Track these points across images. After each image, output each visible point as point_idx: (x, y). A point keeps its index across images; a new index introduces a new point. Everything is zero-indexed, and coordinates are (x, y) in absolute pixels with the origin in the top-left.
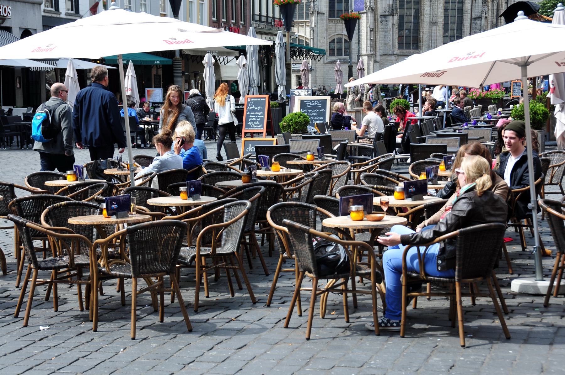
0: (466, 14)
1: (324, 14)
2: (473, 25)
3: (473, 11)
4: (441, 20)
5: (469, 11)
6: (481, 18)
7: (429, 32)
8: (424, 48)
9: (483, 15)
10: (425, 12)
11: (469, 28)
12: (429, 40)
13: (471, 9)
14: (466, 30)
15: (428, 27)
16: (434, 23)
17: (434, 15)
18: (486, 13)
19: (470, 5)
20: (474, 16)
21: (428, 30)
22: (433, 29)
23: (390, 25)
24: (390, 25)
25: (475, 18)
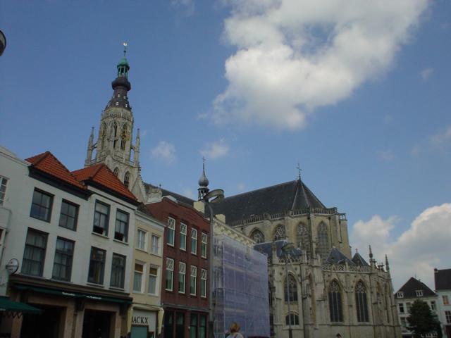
1: (280, 299)
16: (351, 306)
23: (323, 306)
24: (323, 306)
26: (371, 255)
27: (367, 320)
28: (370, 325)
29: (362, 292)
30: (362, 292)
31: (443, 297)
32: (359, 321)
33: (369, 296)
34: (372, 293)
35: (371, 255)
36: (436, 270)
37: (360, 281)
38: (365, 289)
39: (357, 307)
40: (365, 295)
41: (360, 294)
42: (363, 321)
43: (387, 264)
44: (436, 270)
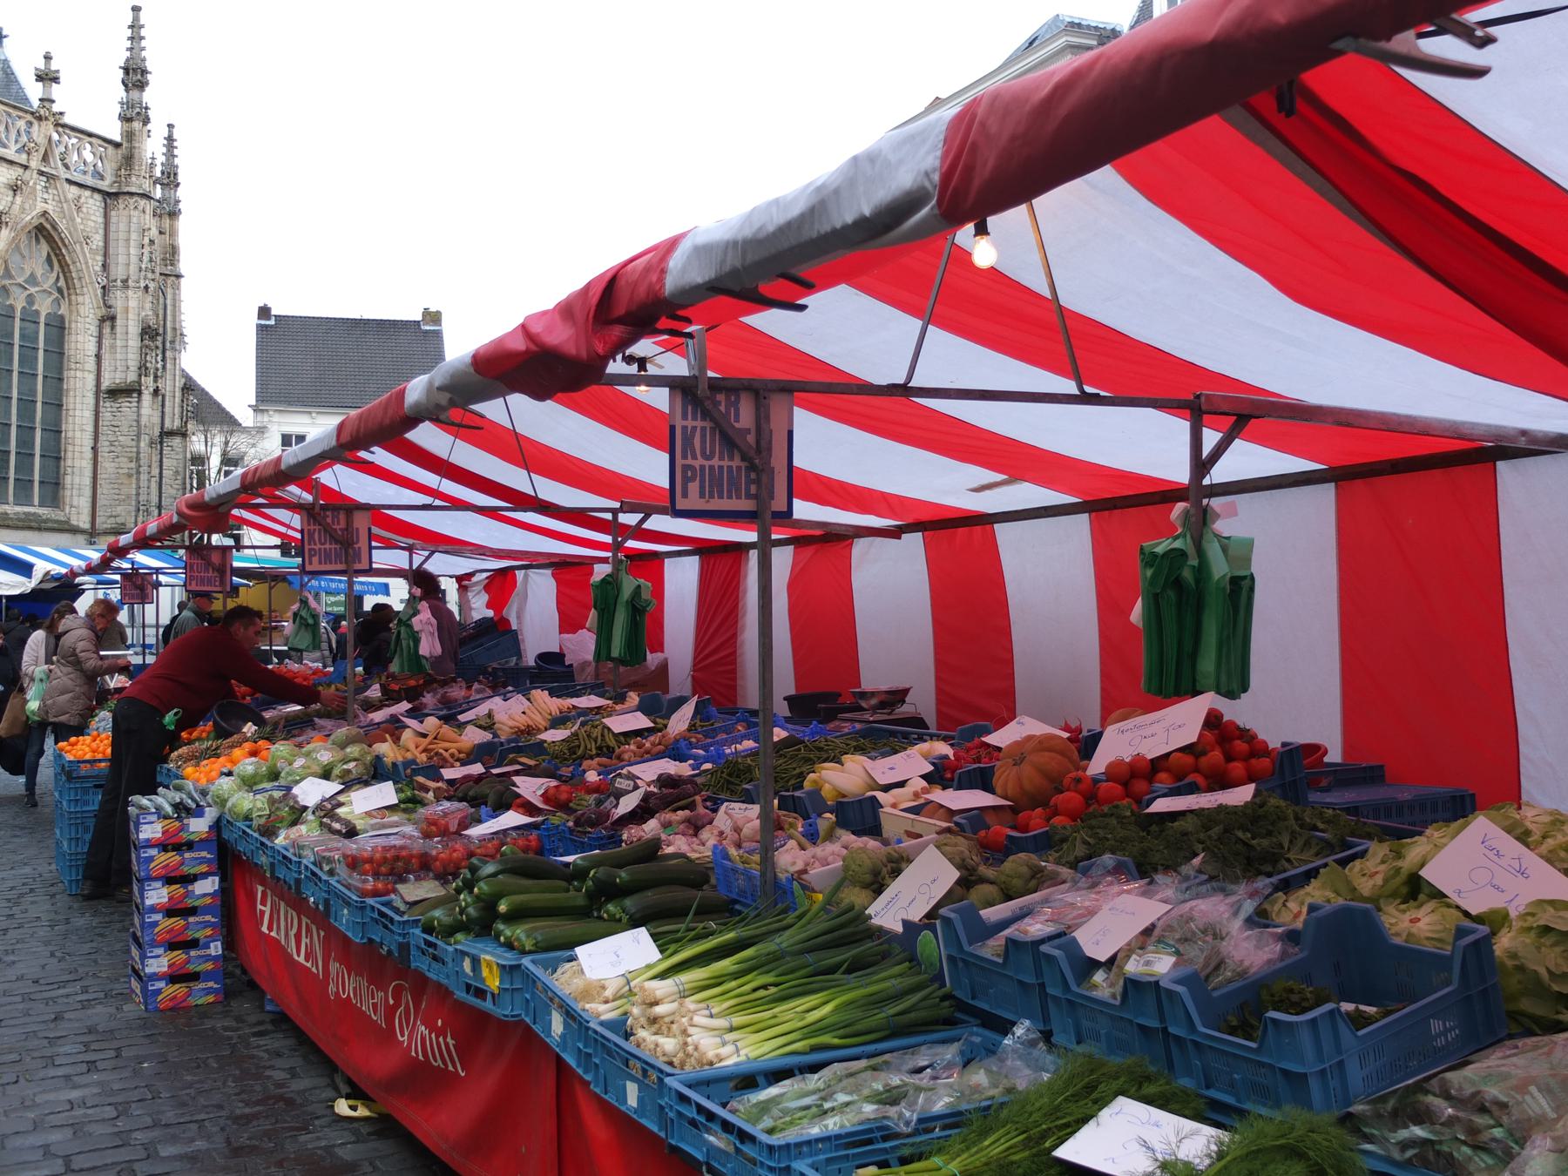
0: (79, 374)
2: (106, 415)
3: (105, 364)
5: (91, 364)
6: (140, 393)
9: (148, 382)
11: (90, 428)
13: (98, 357)
14: (78, 434)
18: (156, 377)
19: (94, 340)
20: (105, 384)
25: (115, 393)
26: (135, 75)
27: (53, 489)
28: (75, 530)
29: (44, 307)
30: (44, 307)
33: (82, 342)
34: (108, 319)
35: (135, 75)
36: (264, 312)
37: (44, 231)
38: (66, 288)
40: (58, 328)
41: (30, 318)
43: (170, 179)
44: (264, 312)
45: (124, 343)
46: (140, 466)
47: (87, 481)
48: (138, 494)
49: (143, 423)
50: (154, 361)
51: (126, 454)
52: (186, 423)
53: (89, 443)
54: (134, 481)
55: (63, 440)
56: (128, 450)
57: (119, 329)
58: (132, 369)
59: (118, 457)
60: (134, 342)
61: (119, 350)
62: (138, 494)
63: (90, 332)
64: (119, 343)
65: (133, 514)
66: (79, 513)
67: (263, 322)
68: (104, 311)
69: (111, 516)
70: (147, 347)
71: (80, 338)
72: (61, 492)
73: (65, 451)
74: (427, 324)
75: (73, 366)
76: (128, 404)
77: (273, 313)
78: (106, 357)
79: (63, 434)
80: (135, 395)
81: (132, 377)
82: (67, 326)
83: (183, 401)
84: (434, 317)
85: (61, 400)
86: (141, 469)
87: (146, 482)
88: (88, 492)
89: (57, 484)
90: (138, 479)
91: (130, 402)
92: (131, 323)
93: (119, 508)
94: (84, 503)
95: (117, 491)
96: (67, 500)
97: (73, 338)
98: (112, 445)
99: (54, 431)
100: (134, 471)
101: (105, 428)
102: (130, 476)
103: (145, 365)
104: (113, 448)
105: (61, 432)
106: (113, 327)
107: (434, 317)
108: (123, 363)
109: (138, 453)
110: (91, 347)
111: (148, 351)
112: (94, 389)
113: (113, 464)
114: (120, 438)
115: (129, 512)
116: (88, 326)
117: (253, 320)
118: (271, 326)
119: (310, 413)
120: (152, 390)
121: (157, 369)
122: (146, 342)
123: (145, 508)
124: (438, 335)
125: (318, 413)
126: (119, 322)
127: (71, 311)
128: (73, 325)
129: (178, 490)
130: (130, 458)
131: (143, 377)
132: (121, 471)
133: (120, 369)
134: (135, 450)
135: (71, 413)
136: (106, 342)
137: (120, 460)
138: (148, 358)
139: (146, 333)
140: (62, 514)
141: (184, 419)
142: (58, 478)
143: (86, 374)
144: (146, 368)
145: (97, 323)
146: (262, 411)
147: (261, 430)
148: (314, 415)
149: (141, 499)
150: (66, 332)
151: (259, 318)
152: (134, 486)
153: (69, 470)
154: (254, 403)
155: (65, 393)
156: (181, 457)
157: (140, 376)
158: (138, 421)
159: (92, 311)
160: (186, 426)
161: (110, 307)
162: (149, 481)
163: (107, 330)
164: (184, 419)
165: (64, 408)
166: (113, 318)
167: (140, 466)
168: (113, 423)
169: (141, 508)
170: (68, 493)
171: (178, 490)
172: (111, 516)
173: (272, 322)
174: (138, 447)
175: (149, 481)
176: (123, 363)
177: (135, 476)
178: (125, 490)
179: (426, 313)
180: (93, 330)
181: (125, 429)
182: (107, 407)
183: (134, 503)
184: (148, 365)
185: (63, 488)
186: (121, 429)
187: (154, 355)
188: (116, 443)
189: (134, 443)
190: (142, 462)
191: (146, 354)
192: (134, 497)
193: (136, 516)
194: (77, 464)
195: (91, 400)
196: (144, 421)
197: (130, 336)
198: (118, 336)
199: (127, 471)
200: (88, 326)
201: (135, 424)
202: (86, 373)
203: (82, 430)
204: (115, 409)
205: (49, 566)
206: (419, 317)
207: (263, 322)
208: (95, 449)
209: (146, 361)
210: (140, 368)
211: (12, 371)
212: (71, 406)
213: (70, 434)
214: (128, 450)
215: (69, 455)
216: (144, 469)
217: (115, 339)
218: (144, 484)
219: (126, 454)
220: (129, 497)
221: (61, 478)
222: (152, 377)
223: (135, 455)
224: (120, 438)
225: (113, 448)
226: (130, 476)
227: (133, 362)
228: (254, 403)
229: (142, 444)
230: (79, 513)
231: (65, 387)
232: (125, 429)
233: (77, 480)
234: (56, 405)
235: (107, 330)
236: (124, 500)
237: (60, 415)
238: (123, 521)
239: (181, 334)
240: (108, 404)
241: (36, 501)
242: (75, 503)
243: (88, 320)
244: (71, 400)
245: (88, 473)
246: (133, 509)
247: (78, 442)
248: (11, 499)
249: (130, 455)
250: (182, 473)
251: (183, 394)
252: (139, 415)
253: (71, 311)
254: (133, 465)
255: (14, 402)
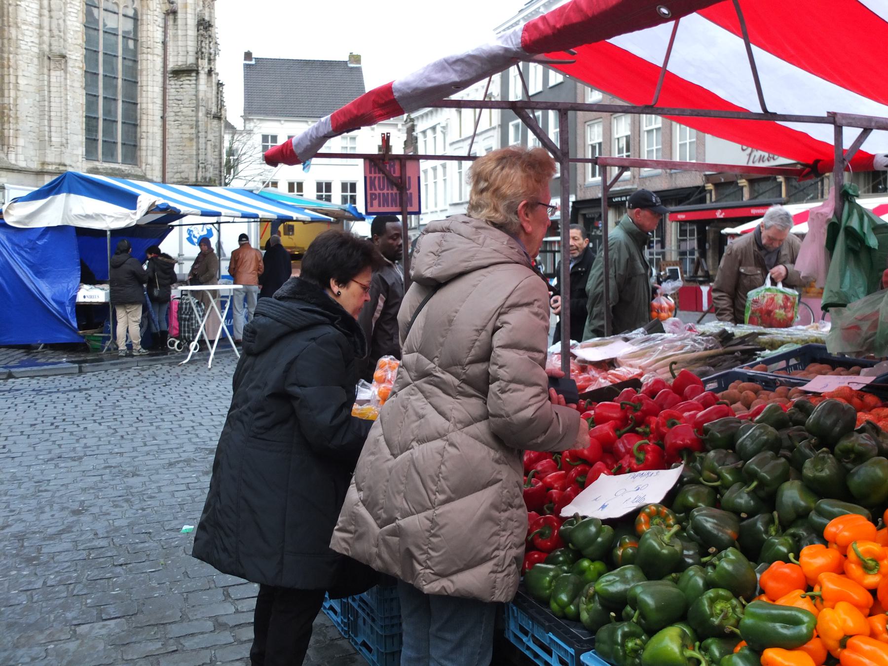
0: (150, 57)
2: (171, 91)
3: (170, 50)
4: (76, 57)
5: (159, 49)
6: (198, 73)
7: (40, 90)
8: (21, 142)
9: (204, 64)
10: (22, 15)
11: (159, 101)
12: (41, 117)
13: (164, 43)
14: (150, 106)
15: (33, 69)
17: (56, 32)
18: (210, 60)
19: (160, 30)
20: (171, 66)
21: (34, 82)
22: (53, 79)
25: (178, 73)
31: (265, 138)
32: (90, 153)
36: (248, 56)
39: (90, 75)
42: (110, 154)
44: (248, 56)
45: (184, 33)
46: (199, 132)
47: (158, 144)
48: (198, 155)
49: (200, 97)
50: (207, 47)
51: (187, 122)
52: (220, 109)
53: (158, 113)
54: (194, 144)
55: (139, 111)
56: (190, 119)
57: (180, 22)
58: (191, 53)
59: (181, 125)
60: (192, 32)
61: (180, 38)
62: (198, 155)
63: (157, 23)
64: (180, 32)
65: (195, 170)
66: (152, 170)
67: (248, 62)
68: (168, 7)
69: (177, 172)
70: (202, 35)
71: (150, 28)
72: (138, 153)
73: (141, 119)
74: (352, 63)
75: (145, 50)
76: (188, 82)
77: (254, 56)
78: (170, 44)
79: (139, 106)
80: (194, 74)
81: (191, 60)
82: (139, 18)
83: (218, 93)
84: (356, 59)
85: (136, 78)
86: (200, 134)
87: (204, 145)
88: (159, 152)
89: (135, 146)
90: (198, 143)
91: (190, 80)
92: (189, 16)
93: (183, 166)
94: (156, 161)
95: (181, 152)
96: (144, 160)
97: (145, 28)
98: (176, 115)
99: (132, 104)
100: (194, 136)
101: (171, 102)
102: (191, 140)
103: (201, 50)
104: (177, 118)
105: (137, 104)
106: (175, 20)
107: (356, 59)
108: (184, 49)
109: (197, 121)
110: (158, 35)
111: (203, 39)
112: (162, 70)
113: (178, 130)
114: (184, 110)
115: (192, 169)
116: (156, 18)
117: (242, 61)
118: (253, 65)
119: (280, 121)
120: (206, 70)
121: (210, 54)
122: (201, 32)
123: (203, 165)
124: (359, 70)
125: (286, 121)
126: (180, 15)
127: (142, 6)
128: (145, 17)
129: (216, 159)
130: (190, 125)
131: (200, 60)
132: (184, 136)
133: (181, 53)
134: (194, 119)
135: (144, 88)
136: (170, 32)
137: (183, 127)
138: (203, 44)
139: (201, 24)
140: (140, 170)
141: (219, 107)
142: (136, 141)
143: (156, 58)
144: (202, 53)
145: (163, 16)
146: (250, 120)
147: (250, 132)
148: (282, 122)
149: (200, 158)
150: (139, 23)
151: (245, 59)
152: (194, 148)
153: (144, 135)
154: (243, 114)
155: (139, 73)
156: (217, 134)
157: (197, 59)
158: (196, 96)
159: (159, 6)
160: (220, 112)
161: (172, 3)
162: (206, 144)
163: (170, 22)
164: (219, 107)
165: (139, 84)
166: (174, 13)
167: (199, 132)
168: (178, 97)
169: (201, 165)
170: (144, 153)
171: (216, 159)
172: (177, 172)
173: (253, 62)
174: (197, 116)
175: (206, 144)
176: (184, 49)
177: (195, 140)
178: (187, 151)
179: (351, 56)
180: (160, 21)
181: (186, 102)
182: (172, 83)
183: (194, 161)
184: (203, 50)
185: (140, 150)
186: (183, 102)
187: (207, 42)
188: (180, 114)
189: (193, 113)
190: (200, 129)
191: (202, 41)
192: (195, 157)
193: (197, 172)
194: (150, 130)
195: (159, 78)
196: (201, 95)
197: (188, 26)
198: (179, 27)
199: (189, 136)
200: (156, 18)
201: (194, 98)
202: (155, 56)
203: (153, 103)
204: (178, 86)
205: (153, 199)
206: (347, 59)
207: (248, 62)
208: (163, 118)
209: (202, 47)
210: (197, 53)
211: (98, 52)
212: (144, 83)
213: (144, 106)
214: (190, 119)
215: (144, 122)
216: (202, 134)
217: (177, 29)
218: (202, 146)
219: (187, 122)
220: (191, 156)
221: (138, 141)
222: (206, 60)
223: (194, 123)
224: (184, 110)
225: (177, 118)
226: (191, 140)
227: (192, 49)
228: (243, 114)
229: (200, 114)
230: (152, 170)
231: (139, 68)
232: (186, 102)
233: (150, 142)
234: (132, 83)
235: (170, 22)
236: (187, 159)
237: (136, 90)
238: (187, 176)
239: (216, 43)
240: (172, 82)
241: (120, 160)
242: (150, 161)
243: (156, 13)
244: (144, 78)
245: (159, 137)
246: (194, 166)
247: (150, 112)
248: (100, 156)
249: (191, 123)
250: (218, 146)
251: (218, 88)
252: (197, 91)
253: (142, 6)
254: (193, 131)
255: (101, 77)
